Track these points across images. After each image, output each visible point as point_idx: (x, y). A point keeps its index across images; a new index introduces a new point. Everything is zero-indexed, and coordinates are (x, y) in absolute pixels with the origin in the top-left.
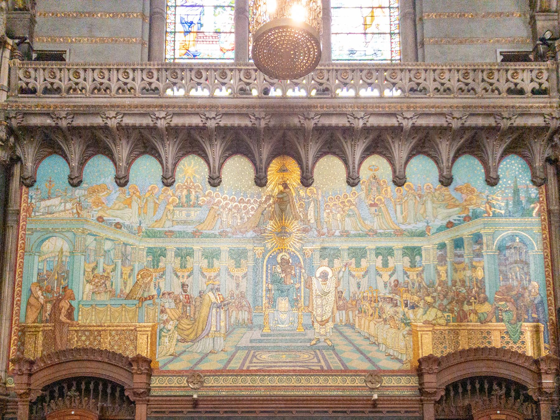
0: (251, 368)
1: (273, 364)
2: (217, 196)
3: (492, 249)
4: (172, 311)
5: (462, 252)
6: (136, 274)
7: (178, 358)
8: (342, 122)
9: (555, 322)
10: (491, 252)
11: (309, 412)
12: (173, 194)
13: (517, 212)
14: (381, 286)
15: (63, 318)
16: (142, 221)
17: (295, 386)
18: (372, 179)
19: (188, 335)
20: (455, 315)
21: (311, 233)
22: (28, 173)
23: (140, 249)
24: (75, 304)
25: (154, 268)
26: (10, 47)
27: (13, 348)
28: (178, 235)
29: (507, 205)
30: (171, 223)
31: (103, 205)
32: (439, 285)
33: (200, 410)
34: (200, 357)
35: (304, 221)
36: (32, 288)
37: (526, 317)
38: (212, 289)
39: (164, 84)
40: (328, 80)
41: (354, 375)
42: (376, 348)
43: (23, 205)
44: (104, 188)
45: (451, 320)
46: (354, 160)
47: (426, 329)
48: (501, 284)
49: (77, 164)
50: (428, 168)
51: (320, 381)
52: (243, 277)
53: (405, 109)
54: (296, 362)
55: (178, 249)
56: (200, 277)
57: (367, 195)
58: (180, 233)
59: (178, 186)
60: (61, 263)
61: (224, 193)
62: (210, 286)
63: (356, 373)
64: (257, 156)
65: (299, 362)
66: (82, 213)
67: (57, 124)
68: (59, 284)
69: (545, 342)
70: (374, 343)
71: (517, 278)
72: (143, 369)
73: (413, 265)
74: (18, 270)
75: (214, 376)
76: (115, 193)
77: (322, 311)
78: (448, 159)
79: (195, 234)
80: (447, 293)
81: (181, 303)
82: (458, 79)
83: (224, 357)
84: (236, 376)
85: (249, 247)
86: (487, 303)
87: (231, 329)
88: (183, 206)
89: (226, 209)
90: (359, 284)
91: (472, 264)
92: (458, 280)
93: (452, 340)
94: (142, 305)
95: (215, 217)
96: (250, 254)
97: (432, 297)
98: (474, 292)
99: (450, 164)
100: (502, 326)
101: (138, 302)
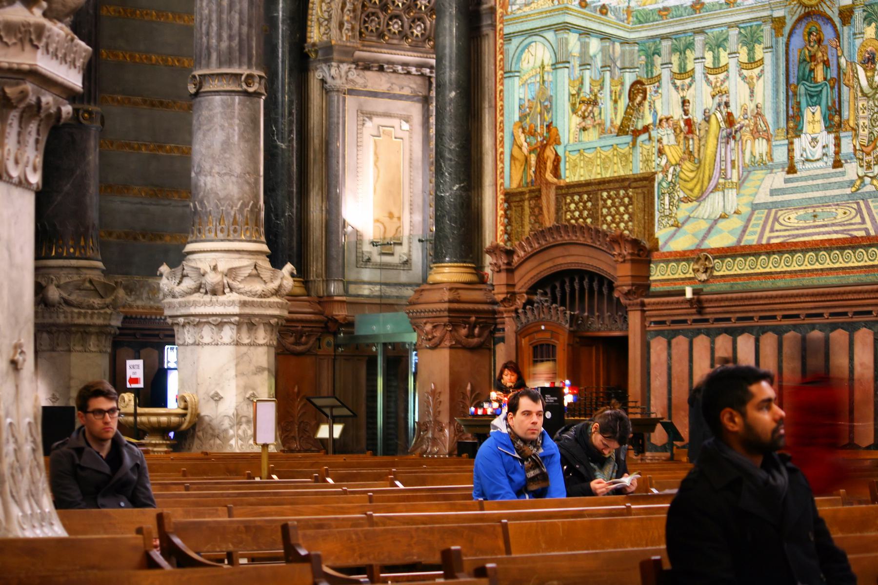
0: (773, 241)
19: (691, 190)
24: (560, 150)
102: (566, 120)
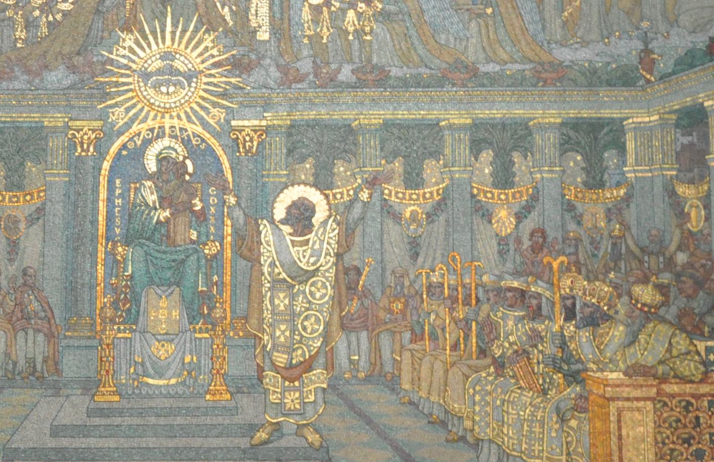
14: (488, 249)
21: (257, 76)
32: (680, 248)
35: (235, 35)
47: (638, 393)
52: (32, 221)
70: (463, 438)
77: (293, 330)
85: (55, 119)
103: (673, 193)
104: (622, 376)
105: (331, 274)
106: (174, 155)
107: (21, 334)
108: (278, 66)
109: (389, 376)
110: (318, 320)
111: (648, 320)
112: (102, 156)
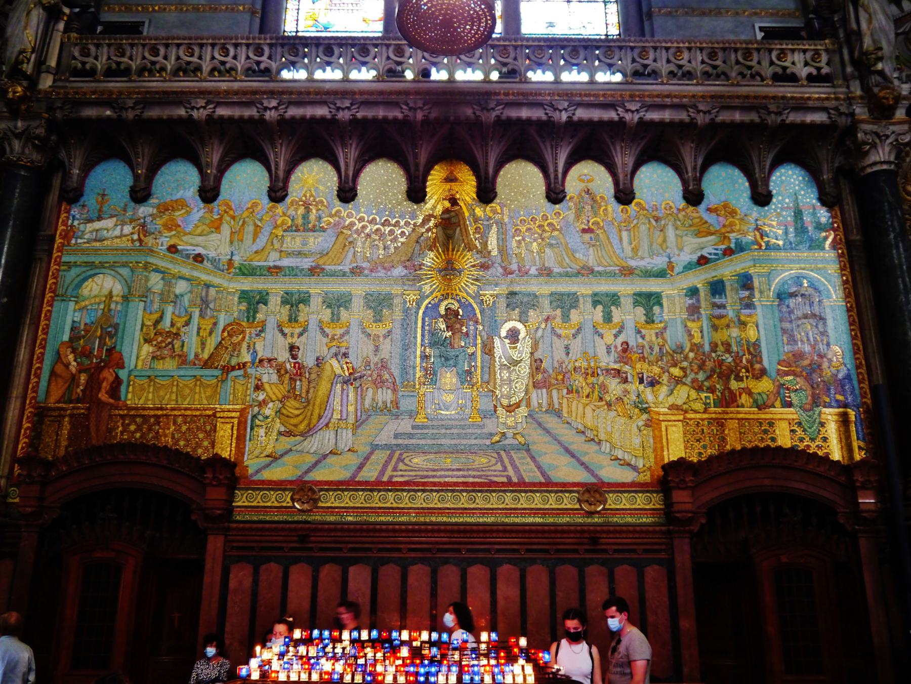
0: (395, 479)
1: (431, 473)
2: (349, 216)
3: (768, 296)
4: (273, 386)
5: (723, 301)
6: (220, 331)
7: (279, 461)
8: (537, 114)
9: (871, 406)
10: (767, 301)
11: (488, 550)
12: (283, 213)
13: (801, 242)
14: (601, 350)
15: (103, 396)
16: (235, 252)
17: (466, 509)
18: (583, 194)
19: (296, 426)
20: (717, 396)
22: (74, 182)
23: (229, 293)
24: (123, 374)
25: (248, 321)
26: (65, 18)
27: (23, 441)
28: (288, 272)
29: (786, 233)
30: (278, 254)
31: (179, 229)
32: (691, 350)
33: (310, 545)
34: (314, 460)
36: (61, 349)
37: (828, 400)
38: (336, 355)
39: (278, 63)
40: (515, 59)
41: (561, 491)
42: (596, 447)
43: (61, 228)
44: (181, 204)
45: (712, 405)
46: (556, 167)
47: (673, 418)
48: (786, 350)
49: (144, 171)
50: (666, 179)
51: (507, 501)
52: (385, 337)
53: (627, 98)
54: (468, 470)
55: (287, 293)
56: (319, 336)
57: (578, 217)
58: (291, 269)
59: (292, 202)
60: (107, 313)
61: (359, 212)
62: (333, 350)
63: (565, 487)
64: (410, 158)
65: (474, 470)
66: (146, 240)
67: (120, 116)
68: (102, 343)
69: (858, 439)
70: (593, 440)
71: (808, 340)
72: (221, 477)
73: (650, 320)
74: (43, 323)
75: (335, 490)
76: (198, 211)
77: (510, 389)
78: (694, 168)
79: (314, 271)
80: (704, 362)
81: (288, 375)
82: (702, 60)
83: (353, 461)
84: (371, 490)
85: (397, 290)
86: (765, 378)
87: (364, 417)
88: (297, 230)
89: (363, 235)
90: (567, 348)
91: (739, 320)
92: (719, 343)
93: (714, 436)
94: (227, 378)
95: (345, 245)
96: (396, 301)
97: (681, 368)
98: (744, 361)
99: (698, 175)
100: (791, 413)
101: (221, 372)
102: (135, 347)
103: (686, 326)
104: (667, 410)
105: (528, 362)
106: (453, 307)
107: (380, 390)
108: (501, 267)
109: (557, 410)
110: (522, 383)
111: (678, 384)
112: (419, 307)
